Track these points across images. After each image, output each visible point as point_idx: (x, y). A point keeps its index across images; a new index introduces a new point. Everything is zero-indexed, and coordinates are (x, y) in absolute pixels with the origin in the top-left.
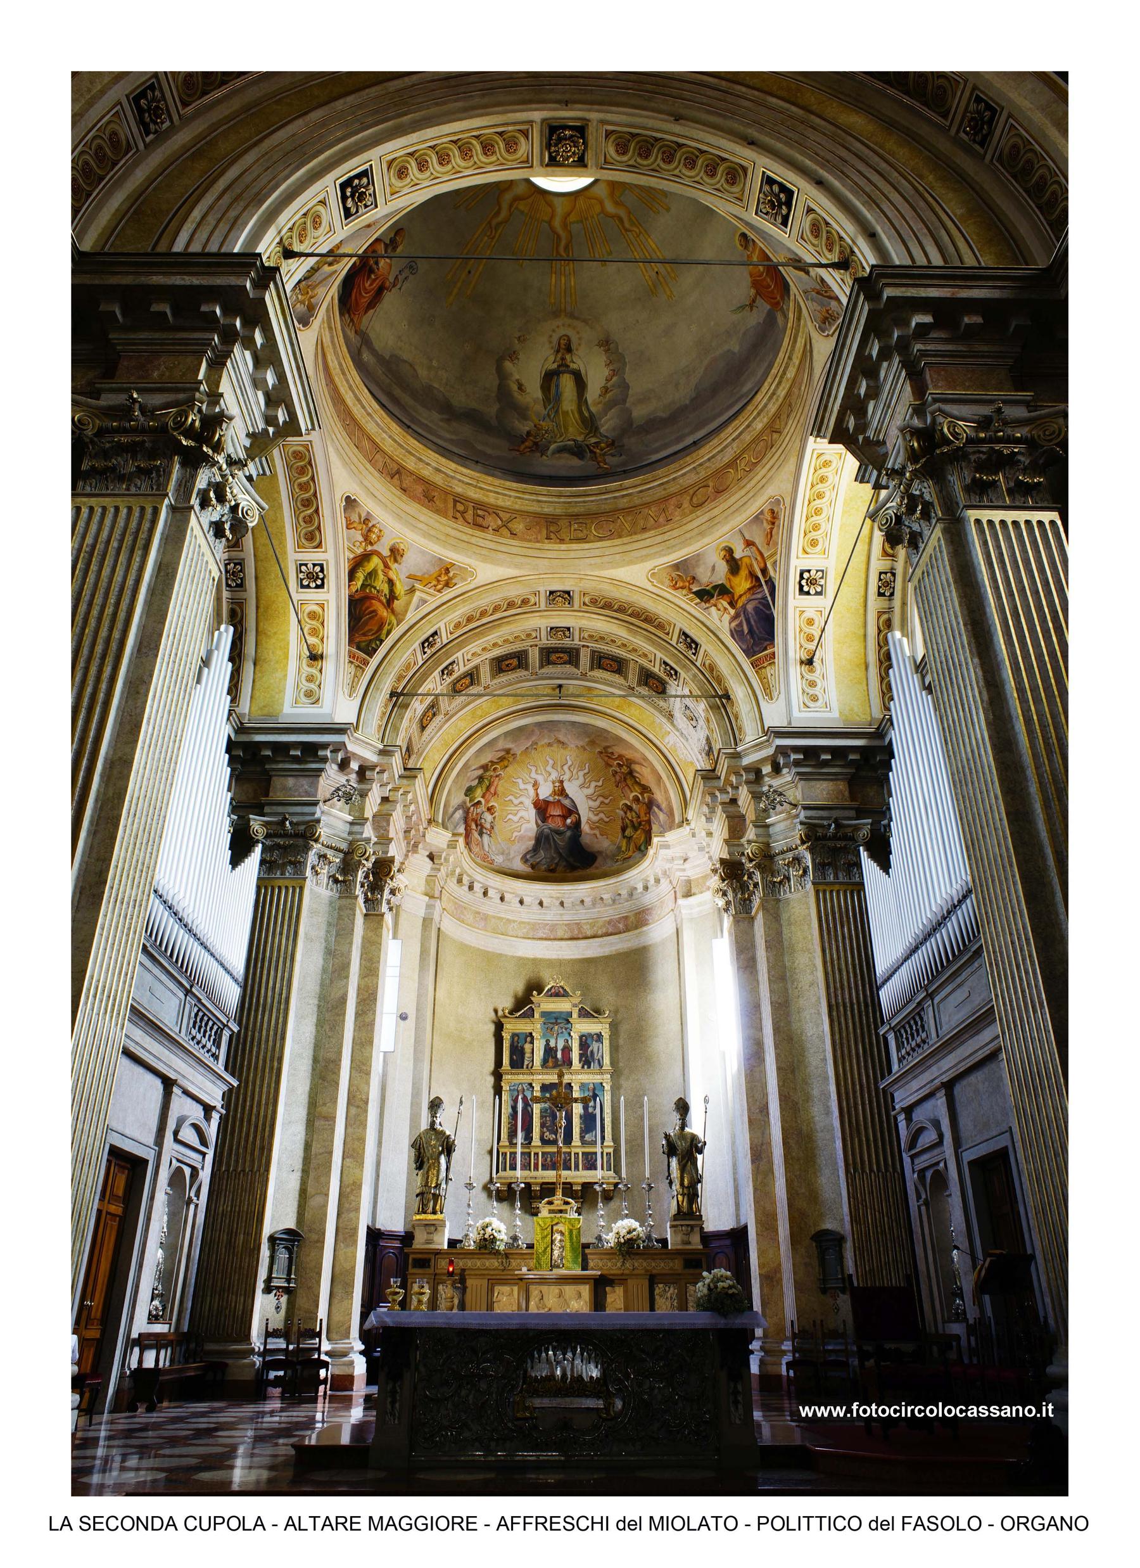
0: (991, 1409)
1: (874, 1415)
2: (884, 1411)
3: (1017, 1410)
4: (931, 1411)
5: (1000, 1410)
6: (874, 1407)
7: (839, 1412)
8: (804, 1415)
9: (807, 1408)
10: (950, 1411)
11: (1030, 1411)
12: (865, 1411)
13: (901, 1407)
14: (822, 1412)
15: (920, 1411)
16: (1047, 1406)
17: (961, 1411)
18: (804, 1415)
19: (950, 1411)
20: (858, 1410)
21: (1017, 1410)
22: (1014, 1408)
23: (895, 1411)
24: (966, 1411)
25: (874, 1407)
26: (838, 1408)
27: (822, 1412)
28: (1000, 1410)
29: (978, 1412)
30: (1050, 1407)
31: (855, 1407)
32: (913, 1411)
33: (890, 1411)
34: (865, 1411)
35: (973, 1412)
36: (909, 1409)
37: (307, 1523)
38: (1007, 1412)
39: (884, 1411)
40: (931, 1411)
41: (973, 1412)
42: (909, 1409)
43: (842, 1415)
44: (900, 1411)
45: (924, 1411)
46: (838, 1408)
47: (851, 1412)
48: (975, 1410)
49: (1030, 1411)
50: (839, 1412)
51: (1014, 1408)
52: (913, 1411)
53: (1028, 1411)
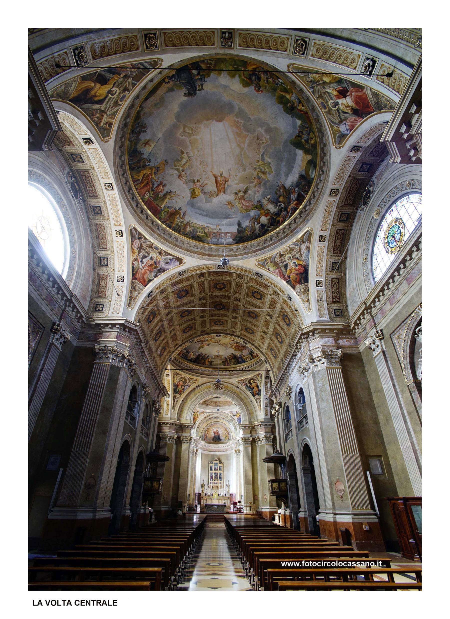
0: (357, 563)
1: (311, 566)
2: (315, 564)
3: (367, 564)
4: (333, 564)
5: (361, 564)
6: (311, 562)
8: (283, 566)
9: (284, 563)
12: (307, 564)
13: (321, 562)
14: (290, 564)
15: (329, 564)
16: (379, 562)
18: (283, 566)
20: (304, 564)
21: (367, 564)
22: (366, 563)
23: (319, 564)
24: (347, 564)
25: (311, 562)
26: (297, 563)
28: (361, 564)
29: (352, 564)
31: (303, 563)
32: (326, 564)
34: (307, 564)
36: (325, 563)
37: (61, 603)
39: (315, 564)
40: (333, 564)
42: (325, 563)
43: (298, 566)
44: (321, 564)
45: (331, 564)
46: (297, 563)
47: (302, 564)
48: (351, 564)
51: (366, 563)
52: (326, 564)
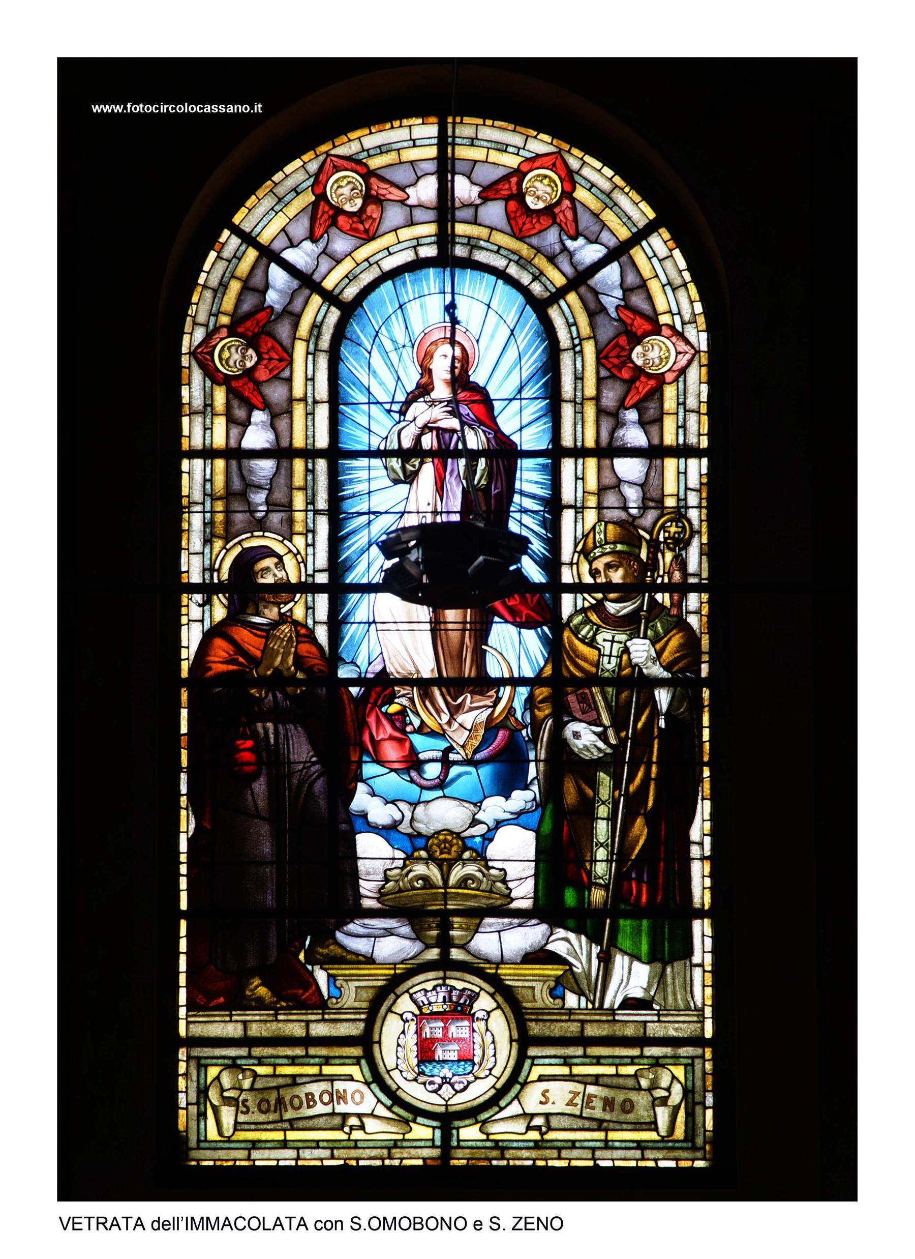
2: (148, 109)
4: (180, 109)
5: (226, 108)
6: (141, 106)
7: (118, 109)
10: (192, 109)
11: (246, 109)
12: (136, 109)
14: (107, 109)
15: (173, 109)
17: (200, 109)
19: (192, 109)
23: (156, 109)
24: (203, 108)
25: (141, 106)
27: (107, 109)
28: (226, 108)
30: (260, 106)
31: (129, 106)
32: (168, 108)
33: (153, 109)
34: (136, 109)
35: (208, 109)
38: (231, 109)
39: (148, 109)
40: (180, 109)
41: (208, 109)
44: (159, 109)
45: (175, 109)
49: (246, 109)
50: (118, 109)
53: (244, 109)
